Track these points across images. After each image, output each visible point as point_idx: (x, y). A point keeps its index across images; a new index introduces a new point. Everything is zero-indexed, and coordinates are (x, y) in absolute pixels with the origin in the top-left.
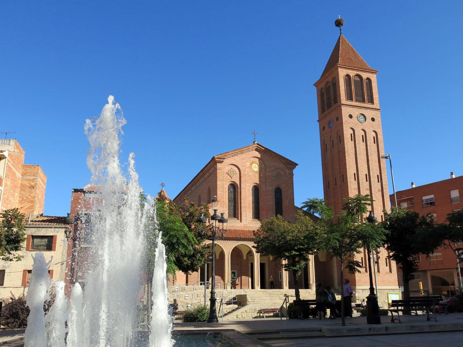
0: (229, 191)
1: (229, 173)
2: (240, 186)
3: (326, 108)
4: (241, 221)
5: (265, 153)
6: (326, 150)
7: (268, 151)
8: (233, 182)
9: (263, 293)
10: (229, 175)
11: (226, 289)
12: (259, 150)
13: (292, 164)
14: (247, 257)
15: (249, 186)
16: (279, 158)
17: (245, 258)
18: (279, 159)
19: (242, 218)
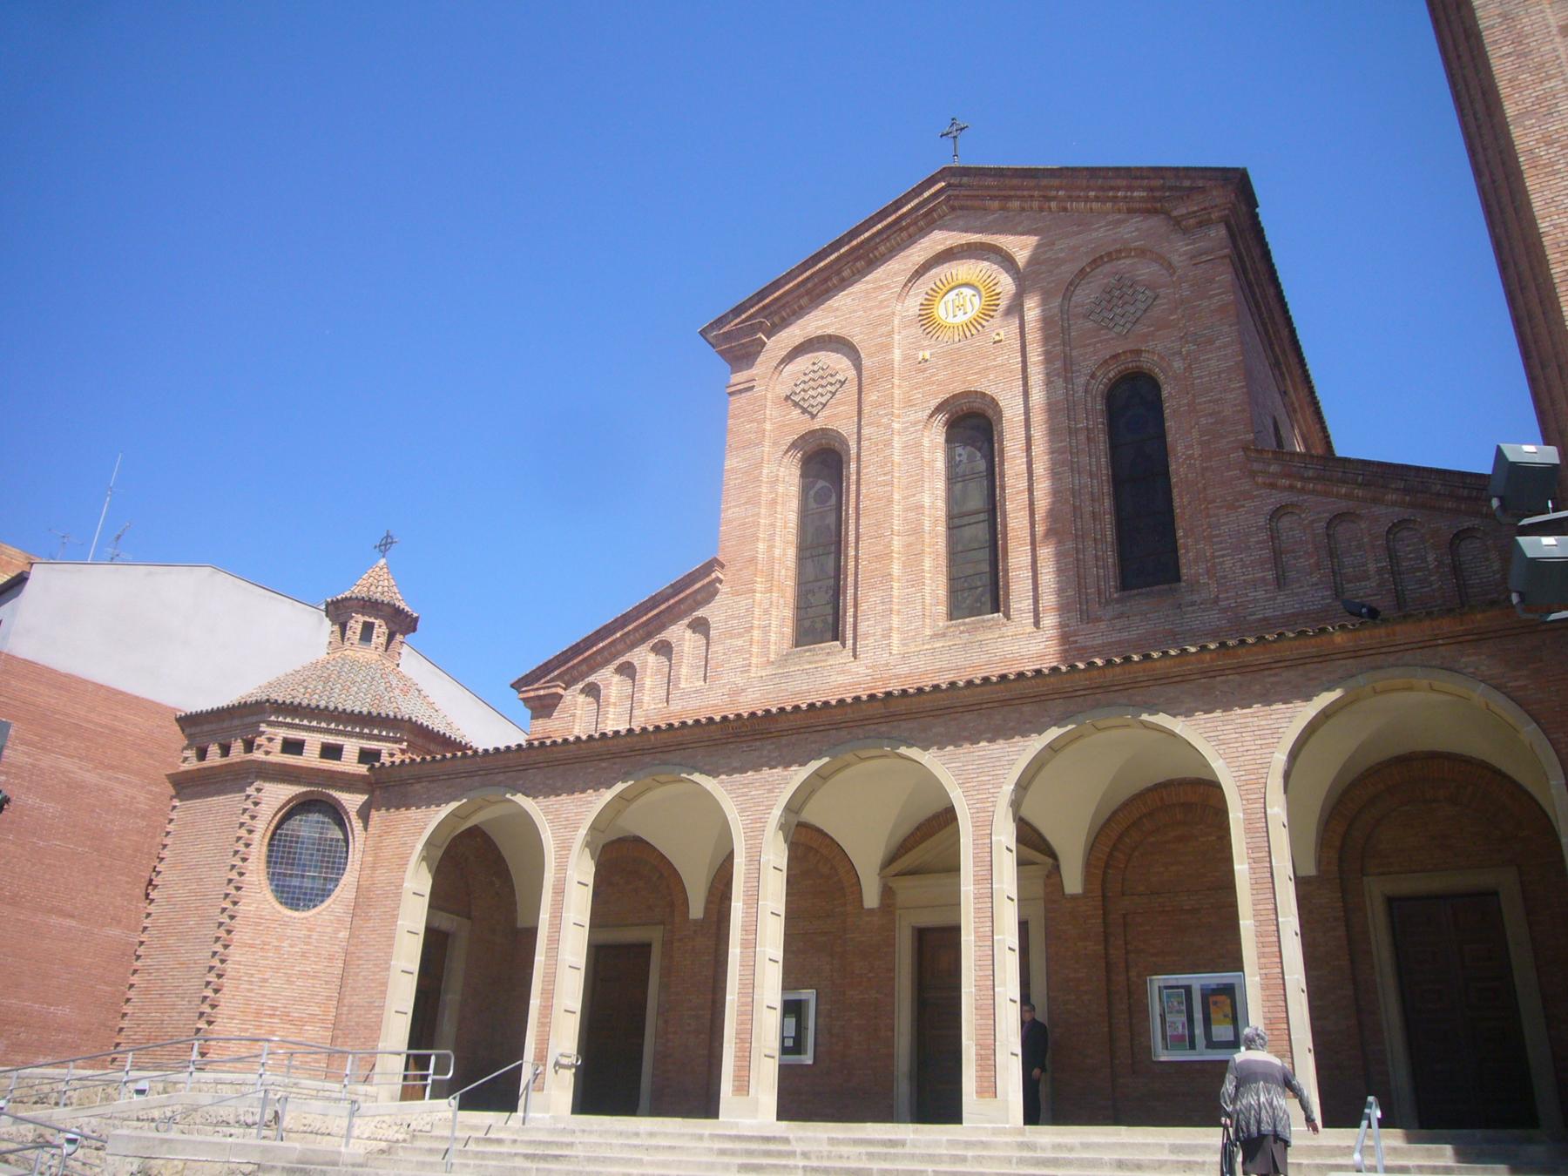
0: (812, 493)
4: (855, 656)
5: (1008, 198)
7: (1015, 181)
9: (722, 1152)
10: (796, 404)
11: (520, 1113)
13: (1200, 183)
14: (887, 892)
15: (915, 424)
16: (1102, 189)
17: (871, 898)
18: (1101, 194)
19: (862, 628)
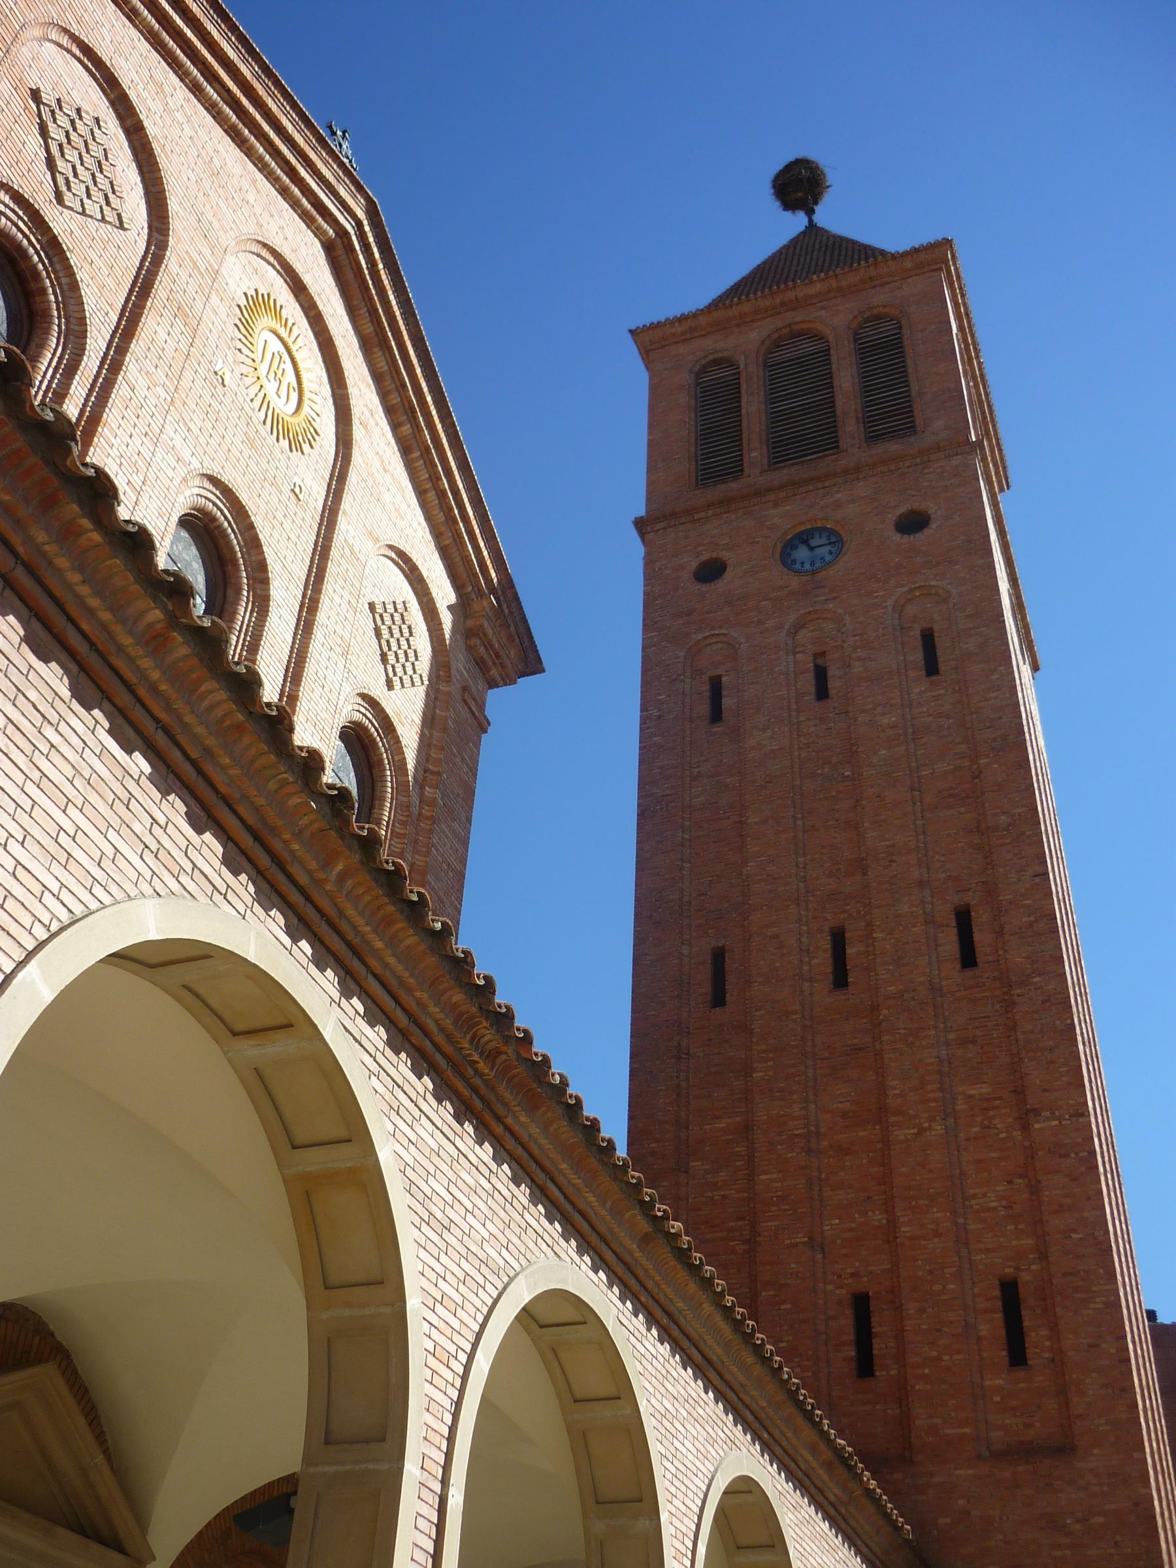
1: (63, 121)
2: (113, 363)
3: (755, 453)
6: (716, 715)
8: (53, 246)
12: (350, 276)
